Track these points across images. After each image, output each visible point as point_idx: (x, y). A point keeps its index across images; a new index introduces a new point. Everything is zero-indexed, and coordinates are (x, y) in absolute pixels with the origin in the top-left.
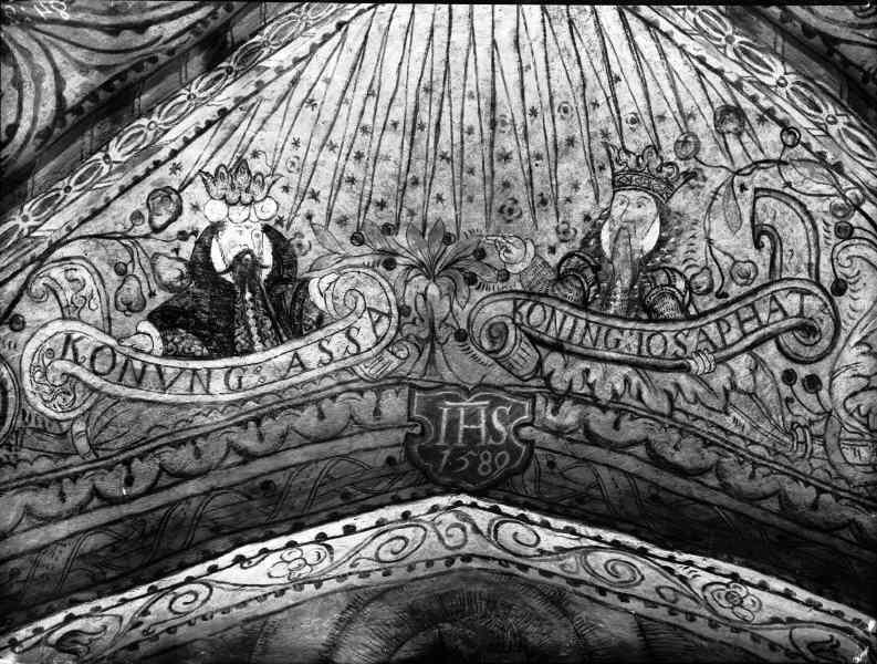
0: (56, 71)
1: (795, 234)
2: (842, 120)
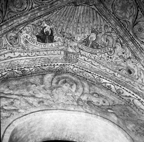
0: (32, 3)
1: (111, 41)
2: (119, 28)
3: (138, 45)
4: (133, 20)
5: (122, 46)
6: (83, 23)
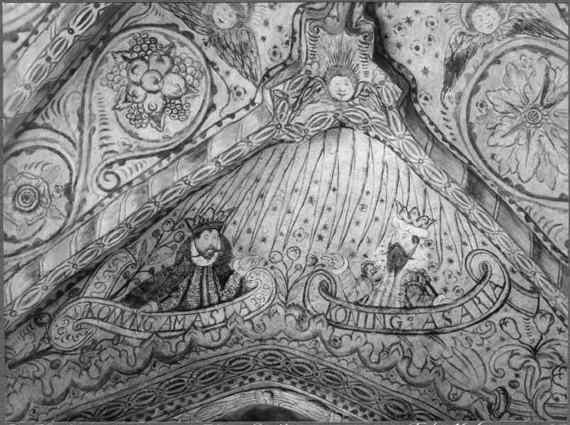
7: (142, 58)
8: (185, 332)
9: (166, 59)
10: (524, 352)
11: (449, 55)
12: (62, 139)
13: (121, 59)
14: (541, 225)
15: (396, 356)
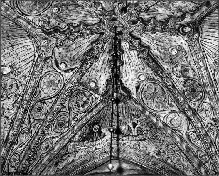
1: (13, 90)
2: (31, 91)
3: (25, 117)
4: (44, 98)
5: (14, 103)
6: (14, 52)
7: (78, 96)
8: (94, 146)
9: (83, 95)
10: (161, 142)
11: (136, 85)
12: (66, 113)
13: (74, 96)
14: (158, 116)
15: (137, 146)
